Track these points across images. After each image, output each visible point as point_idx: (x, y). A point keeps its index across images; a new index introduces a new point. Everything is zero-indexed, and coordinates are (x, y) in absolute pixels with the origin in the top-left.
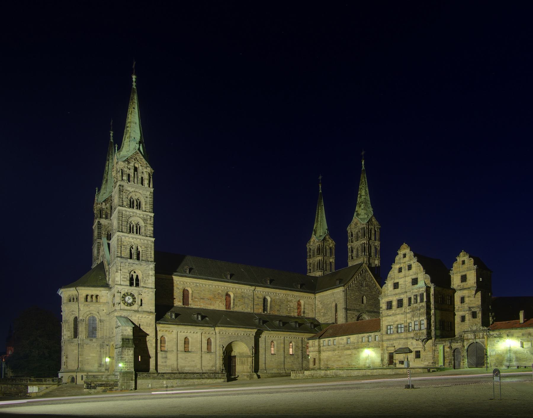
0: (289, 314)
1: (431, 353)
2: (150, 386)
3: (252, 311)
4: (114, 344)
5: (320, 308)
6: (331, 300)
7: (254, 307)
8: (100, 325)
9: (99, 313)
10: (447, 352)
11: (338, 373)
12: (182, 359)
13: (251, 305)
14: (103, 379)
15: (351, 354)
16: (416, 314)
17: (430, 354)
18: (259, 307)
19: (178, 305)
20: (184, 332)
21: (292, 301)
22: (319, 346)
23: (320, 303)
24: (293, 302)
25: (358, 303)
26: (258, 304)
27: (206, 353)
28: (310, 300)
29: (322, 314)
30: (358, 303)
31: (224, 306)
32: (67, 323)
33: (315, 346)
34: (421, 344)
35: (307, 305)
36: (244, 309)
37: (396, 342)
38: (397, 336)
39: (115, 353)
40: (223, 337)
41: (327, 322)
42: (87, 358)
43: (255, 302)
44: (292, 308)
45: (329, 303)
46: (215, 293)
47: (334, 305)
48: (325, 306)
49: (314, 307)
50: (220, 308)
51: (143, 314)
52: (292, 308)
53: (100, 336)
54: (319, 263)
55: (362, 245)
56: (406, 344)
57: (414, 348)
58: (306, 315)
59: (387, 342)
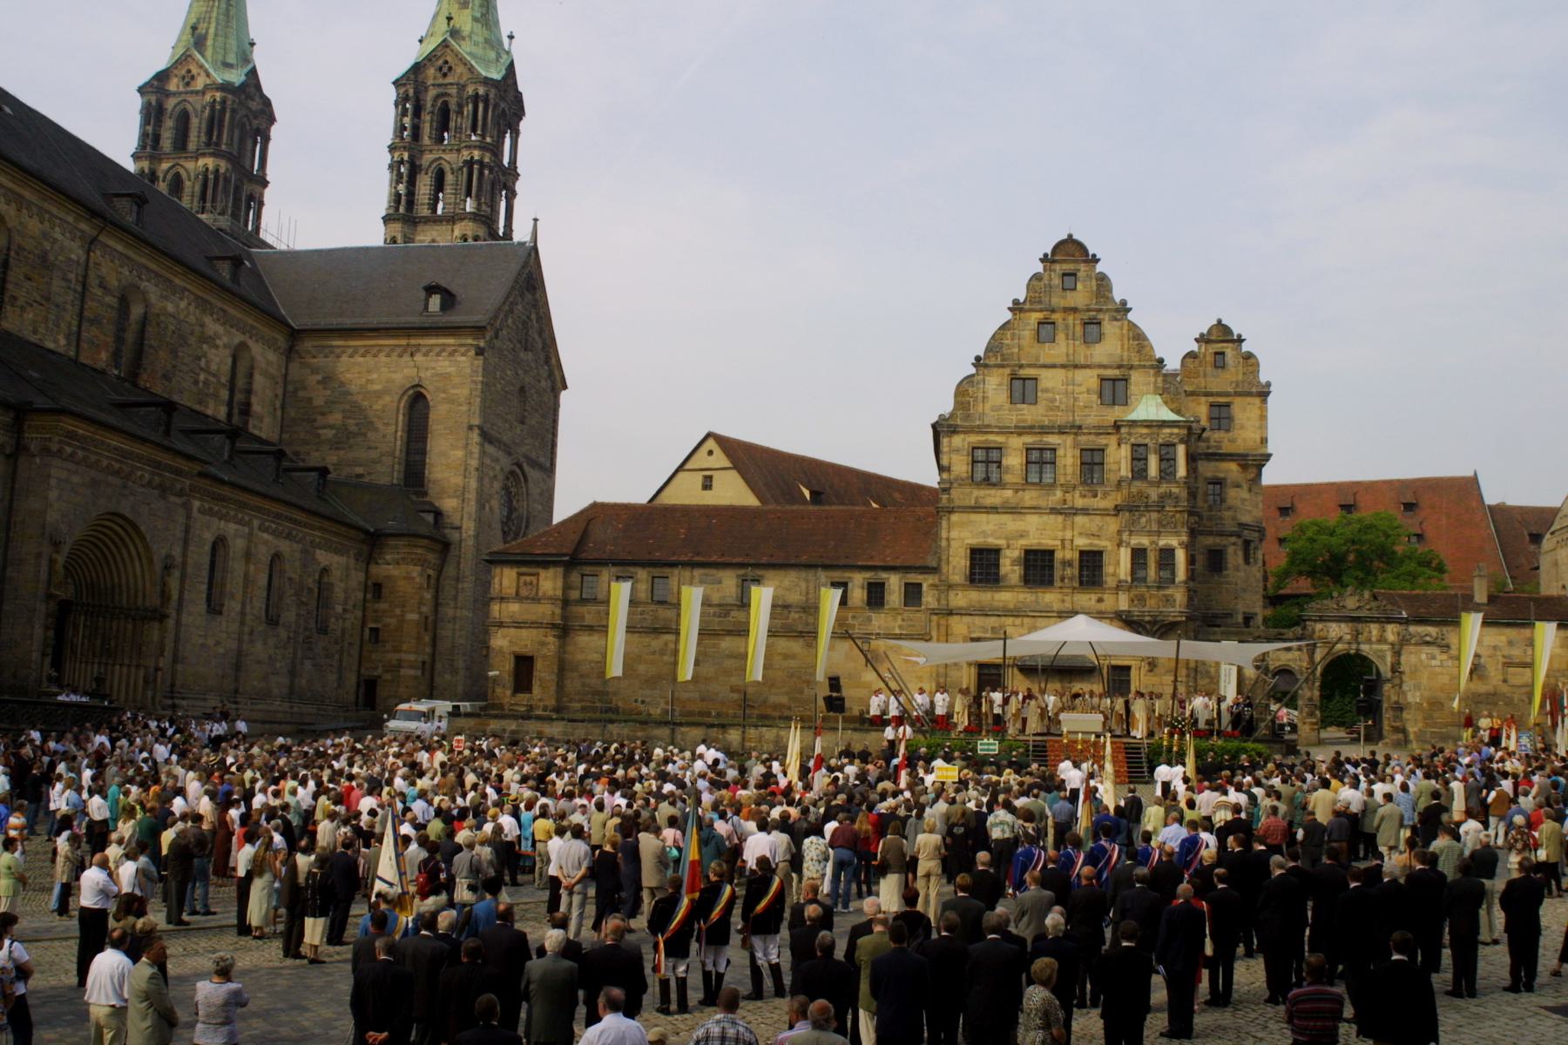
0: (200, 403)
3: (72, 354)
6: (394, 376)
7: (84, 334)
13: (70, 316)
18: (102, 337)
23: (319, 377)
24: (216, 347)
26: (95, 321)
28: (272, 356)
29: (328, 434)
37: (1018, 621)
38: (1021, 597)
41: (359, 476)
43: (89, 304)
44: (214, 375)
45: (377, 387)
49: (280, 392)
59: (966, 619)
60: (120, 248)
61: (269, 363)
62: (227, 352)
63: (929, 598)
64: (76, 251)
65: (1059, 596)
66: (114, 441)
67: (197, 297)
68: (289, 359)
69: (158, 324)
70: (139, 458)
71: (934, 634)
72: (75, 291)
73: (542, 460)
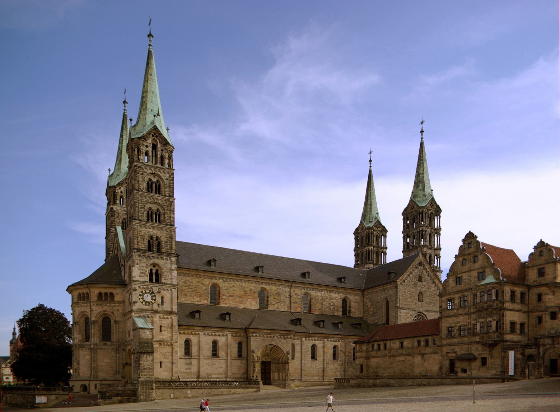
0: (332, 313)
1: (499, 360)
2: (172, 395)
3: (289, 311)
4: (131, 348)
5: (369, 306)
6: (382, 297)
8: (115, 328)
9: (114, 313)
10: (518, 359)
11: (389, 382)
12: (209, 365)
13: (288, 303)
14: (120, 388)
15: (404, 361)
16: (483, 314)
17: (498, 362)
18: (298, 305)
19: (203, 303)
20: (212, 335)
21: (336, 298)
22: (368, 351)
23: (369, 300)
24: (337, 299)
25: (414, 301)
27: (236, 358)
28: (357, 297)
29: (371, 313)
30: (414, 301)
31: (256, 304)
32: (78, 325)
33: (362, 351)
34: (488, 350)
35: (354, 302)
36: (280, 307)
37: (458, 347)
38: (459, 339)
39: (132, 359)
40: (256, 340)
41: (377, 322)
42: (100, 364)
44: (336, 306)
45: (379, 300)
46: (246, 289)
47: (384, 303)
48: (375, 304)
49: (362, 305)
50: (252, 306)
51: (163, 313)
52: (336, 306)
53: (115, 340)
54: (368, 254)
55: (419, 232)
56: (470, 349)
57: (479, 354)
58: (353, 315)
59: (446, 347)
60: (300, 286)
61: (356, 299)
62: (340, 300)
63: (438, 343)
64: (287, 290)
65: (468, 339)
66: (266, 331)
67: (327, 290)
68: (363, 297)
69: (315, 299)
70: (274, 333)
71: (439, 352)
72: (288, 298)
73: (435, 309)
